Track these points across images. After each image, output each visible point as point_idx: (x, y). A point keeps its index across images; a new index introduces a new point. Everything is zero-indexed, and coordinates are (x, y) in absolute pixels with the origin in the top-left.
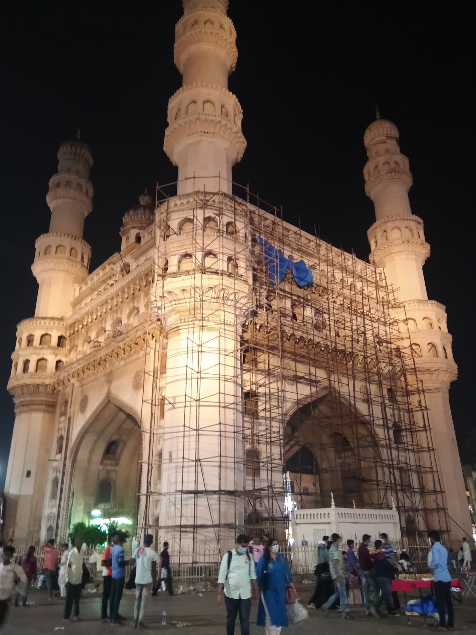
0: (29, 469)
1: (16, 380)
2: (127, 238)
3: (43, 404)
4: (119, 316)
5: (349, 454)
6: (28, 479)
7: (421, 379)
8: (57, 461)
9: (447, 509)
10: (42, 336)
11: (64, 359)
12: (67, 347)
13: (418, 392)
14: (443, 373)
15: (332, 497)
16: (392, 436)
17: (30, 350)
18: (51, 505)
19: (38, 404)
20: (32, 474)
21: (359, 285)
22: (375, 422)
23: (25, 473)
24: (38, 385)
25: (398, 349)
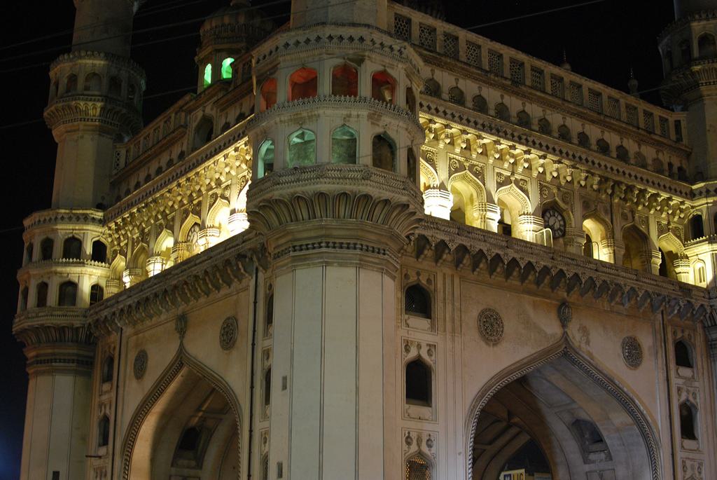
0: (57, 470)
5: (603, 455)
8: (100, 457)
19: (65, 361)
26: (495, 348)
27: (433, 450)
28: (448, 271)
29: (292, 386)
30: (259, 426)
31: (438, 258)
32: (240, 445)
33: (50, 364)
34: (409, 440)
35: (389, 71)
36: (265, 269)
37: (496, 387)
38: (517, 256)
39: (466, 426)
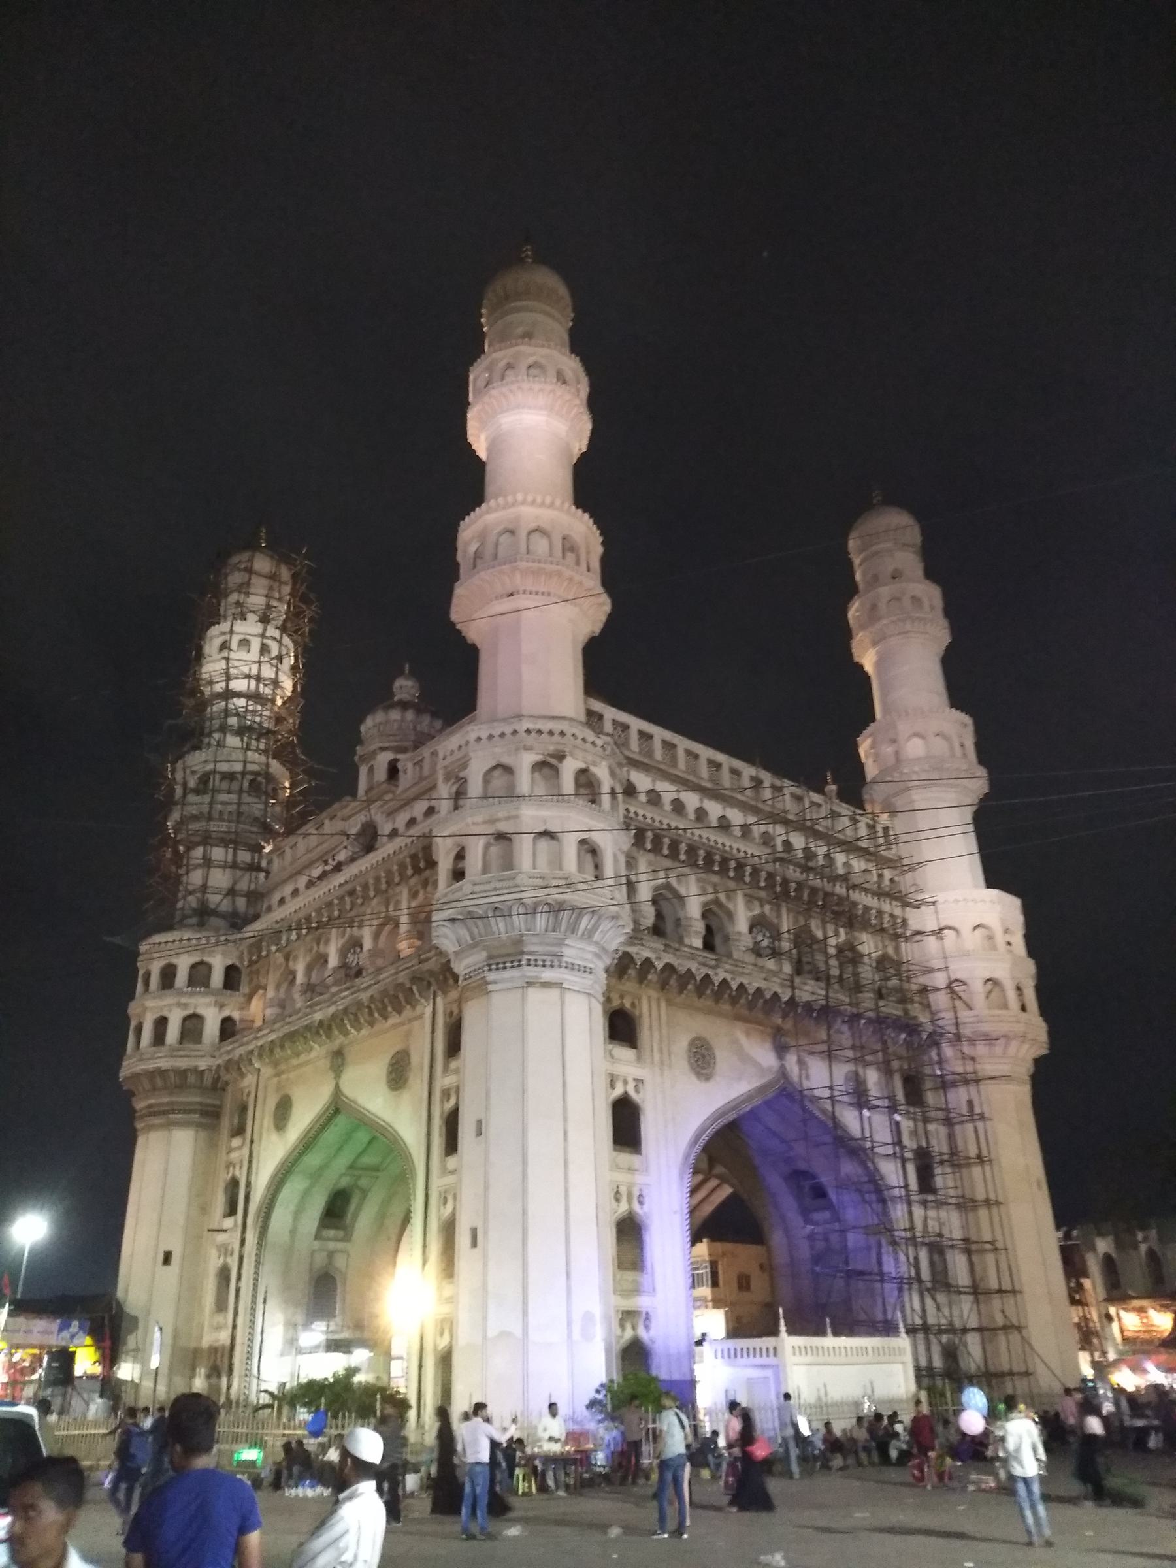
0: (168, 1249)
1: (142, 1060)
2: (371, 770)
3: (195, 1112)
5: (827, 1215)
7: (972, 1054)
9: (1026, 1327)
11: (236, 1015)
12: (245, 989)
13: (966, 1082)
15: (781, 1316)
17: (169, 999)
19: (185, 1112)
20: (175, 1259)
21: (840, 858)
22: (876, 1150)
23: (161, 1257)
24: (185, 1071)
25: (924, 990)
27: (646, 1207)
28: (654, 994)
30: (437, 1183)
31: (642, 976)
33: (166, 1116)
35: (593, 769)
36: (445, 993)
37: (712, 1130)
38: (728, 977)
39: (681, 1178)
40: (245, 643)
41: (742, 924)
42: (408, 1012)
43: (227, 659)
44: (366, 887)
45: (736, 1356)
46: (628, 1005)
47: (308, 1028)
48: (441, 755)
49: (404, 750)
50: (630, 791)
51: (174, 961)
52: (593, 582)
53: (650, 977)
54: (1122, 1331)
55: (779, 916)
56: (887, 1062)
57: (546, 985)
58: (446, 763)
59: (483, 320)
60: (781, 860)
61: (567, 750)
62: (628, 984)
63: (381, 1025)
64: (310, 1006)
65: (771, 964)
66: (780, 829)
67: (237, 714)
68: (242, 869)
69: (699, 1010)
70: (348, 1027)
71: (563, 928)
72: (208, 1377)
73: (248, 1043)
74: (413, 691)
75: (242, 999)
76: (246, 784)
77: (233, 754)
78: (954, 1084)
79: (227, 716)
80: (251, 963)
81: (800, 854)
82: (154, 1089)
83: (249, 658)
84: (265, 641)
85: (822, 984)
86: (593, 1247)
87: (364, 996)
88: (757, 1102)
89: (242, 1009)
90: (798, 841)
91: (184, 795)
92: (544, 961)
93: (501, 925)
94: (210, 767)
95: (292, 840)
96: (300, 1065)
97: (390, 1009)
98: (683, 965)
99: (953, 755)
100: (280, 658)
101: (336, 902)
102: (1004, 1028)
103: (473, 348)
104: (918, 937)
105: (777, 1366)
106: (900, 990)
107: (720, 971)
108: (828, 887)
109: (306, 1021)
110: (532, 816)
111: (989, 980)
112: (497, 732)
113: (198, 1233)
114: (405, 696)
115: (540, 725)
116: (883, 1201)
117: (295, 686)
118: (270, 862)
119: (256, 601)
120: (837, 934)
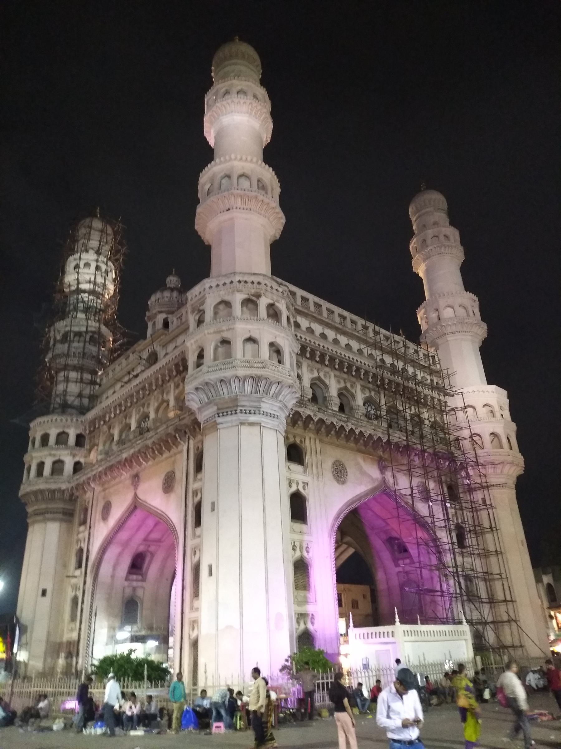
0: (44, 587)
1: (30, 485)
2: (154, 324)
4: (146, 410)
5: (408, 561)
6: (44, 598)
7: (484, 472)
8: (75, 577)
9: (519, 621)
10: (59, 435)
11: (82, 460)
12: (87, 446)
13: (482, 487)
14: (507, 467)
15: (396, 613)
16: (455, 540)
18: (70, 628)
19: (54, 513)
20: (49, 593)
21: (411, 370)
22: (436, 524)
23: (40, 592)
25: (457, 440)
26: (344, 486)
27: (310, 554)
28: (312, 436)
29: (218, 508)
30: (190, 543)
31: (306, 426)
32: (176, 559)
34: (295, 547)
35: (277, 304)
37: (346, 511)
39: (330, 538)
40: (87, 265)
41: (359, 400)
42: (174, 450)
43: (78, 273)
44: (150, 384)
45: (368, 638)
46: (298, 441)
47: (119, 462)
48: (189, 298)
49: (172, 313)
50: (297, 325)
51: (48, 431)
52: (275, 203)
53: (310, 426)
54: (558, 624)
55: (380, 398)
56: (439, 476)
57: (252, 424)
58: (193, 302)
59: (213, 74)
60: (381, 366)
61: (262, 292)
62: (298, 430)
63: (159, 458)
64: (121, 451)
65: (375, 422)
66: (378, 353)
67: (83, 302)
68: (85, 383)
69: (338, 446)
70: (141, 460)
71: (261, 392)
72: (66, 658)
73: (87, 474)
74: (177, 283)
75: (85, 452)
76: (88, 338)
77: (80, 322)
78: (475, 490)
79: (78, 303)
80: (90, 432)
81: (389, 365)
82: (37, 500)
83: (90, 272)
84: (98, 264)
85: (405, 434)
86: (282, 576)
87: (149, 442)
88: (370, 497)
89: (85, 457)
90: (388, 360)
91: (54, 345)
92: (250, 411)
93: (225, 391)
94: (68, 329)
95: (112, 367)
96: (117, 484)
97: (164, 448)
98: (329, 420)
99: (468, 315)
100: (107, 273)
101: (134, 394)
102: (501, 459)
103: (208, 84)
104: (453, 413)
105: (394, 643)
106: (445, 439)
107: (349, 424)
108: (406, 383)
109: (118, 459)
110: (243, 327)
111: (492, 434)
112: (221, 283)
113: (61, 577)
114: (172, 286)
115: (246, 278)
116: (440, 553)
117: (115, 290)
118: (101, 380)
119: (94, 243)
120: (410, 408)
